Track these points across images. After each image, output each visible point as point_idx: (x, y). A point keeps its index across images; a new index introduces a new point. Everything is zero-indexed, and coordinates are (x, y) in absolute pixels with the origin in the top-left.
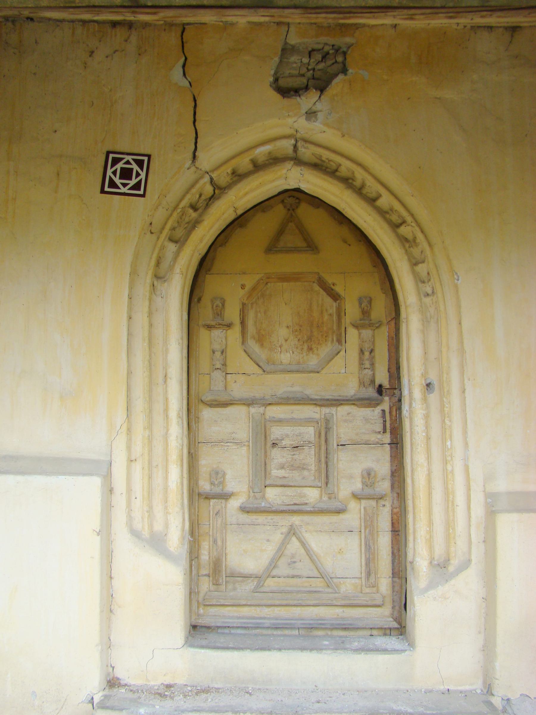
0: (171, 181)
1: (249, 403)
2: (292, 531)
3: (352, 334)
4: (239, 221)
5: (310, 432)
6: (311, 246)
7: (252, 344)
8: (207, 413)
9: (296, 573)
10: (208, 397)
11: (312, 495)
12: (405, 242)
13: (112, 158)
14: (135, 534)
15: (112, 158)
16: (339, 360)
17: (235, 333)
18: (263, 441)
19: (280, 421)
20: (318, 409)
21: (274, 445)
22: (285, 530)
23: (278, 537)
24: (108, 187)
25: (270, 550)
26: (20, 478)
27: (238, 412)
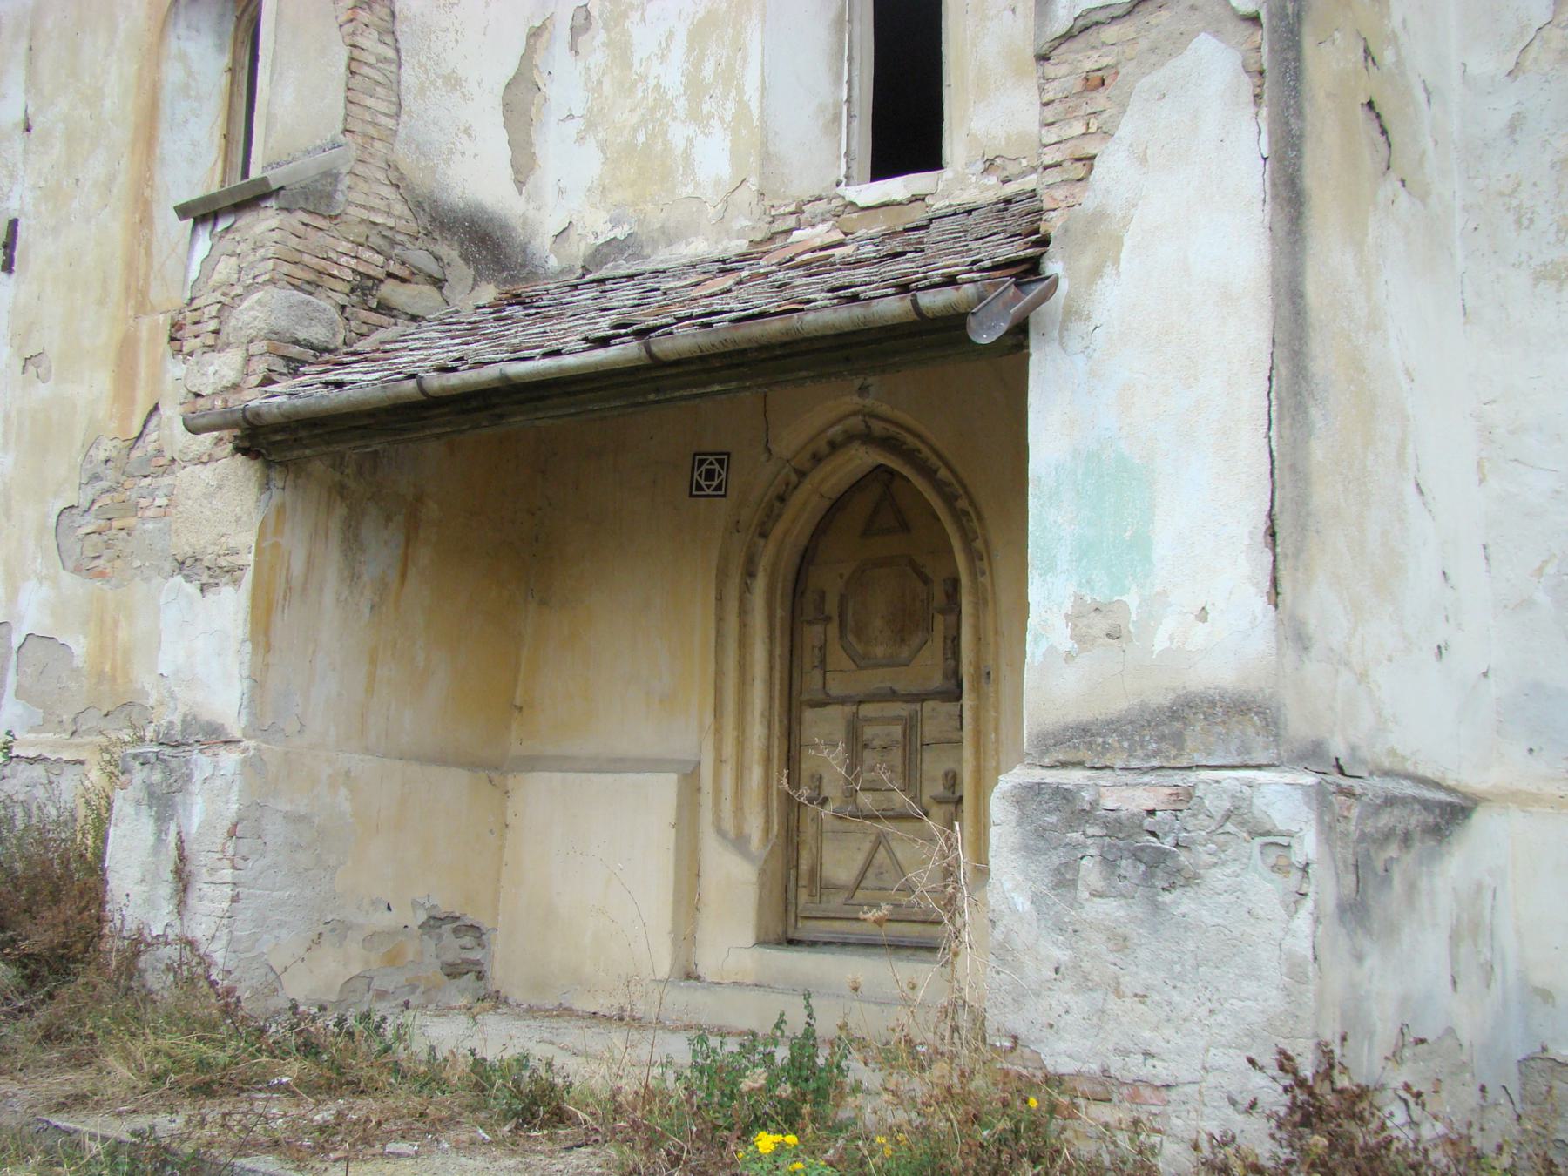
0: (753, 478)
1: (842, 701)
2: (880, 841)
3: (939, 619)
4: (838, 505)
5: (897, 730)
6: (905, 527)
7: (851, 637)
8: (809, 715)
9: (881, 884)
10: (805, 697)
11: (901, 799)
12: (959, 516)
13: (698, 459)
14: (720, 832)
15: (698, 459)
16: (925, 652)
17: (833, 629)
18: (856, 745)
19: (869, 720)
20: (904, 705)
21: (866, 746)
22: (873, 838)
23: (867, 846)
24: (695, 491)
25: (859, 860)
26: (616, 776)
27: (834, 711)
